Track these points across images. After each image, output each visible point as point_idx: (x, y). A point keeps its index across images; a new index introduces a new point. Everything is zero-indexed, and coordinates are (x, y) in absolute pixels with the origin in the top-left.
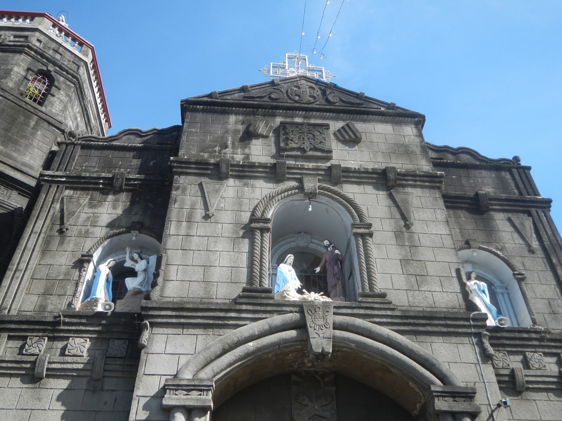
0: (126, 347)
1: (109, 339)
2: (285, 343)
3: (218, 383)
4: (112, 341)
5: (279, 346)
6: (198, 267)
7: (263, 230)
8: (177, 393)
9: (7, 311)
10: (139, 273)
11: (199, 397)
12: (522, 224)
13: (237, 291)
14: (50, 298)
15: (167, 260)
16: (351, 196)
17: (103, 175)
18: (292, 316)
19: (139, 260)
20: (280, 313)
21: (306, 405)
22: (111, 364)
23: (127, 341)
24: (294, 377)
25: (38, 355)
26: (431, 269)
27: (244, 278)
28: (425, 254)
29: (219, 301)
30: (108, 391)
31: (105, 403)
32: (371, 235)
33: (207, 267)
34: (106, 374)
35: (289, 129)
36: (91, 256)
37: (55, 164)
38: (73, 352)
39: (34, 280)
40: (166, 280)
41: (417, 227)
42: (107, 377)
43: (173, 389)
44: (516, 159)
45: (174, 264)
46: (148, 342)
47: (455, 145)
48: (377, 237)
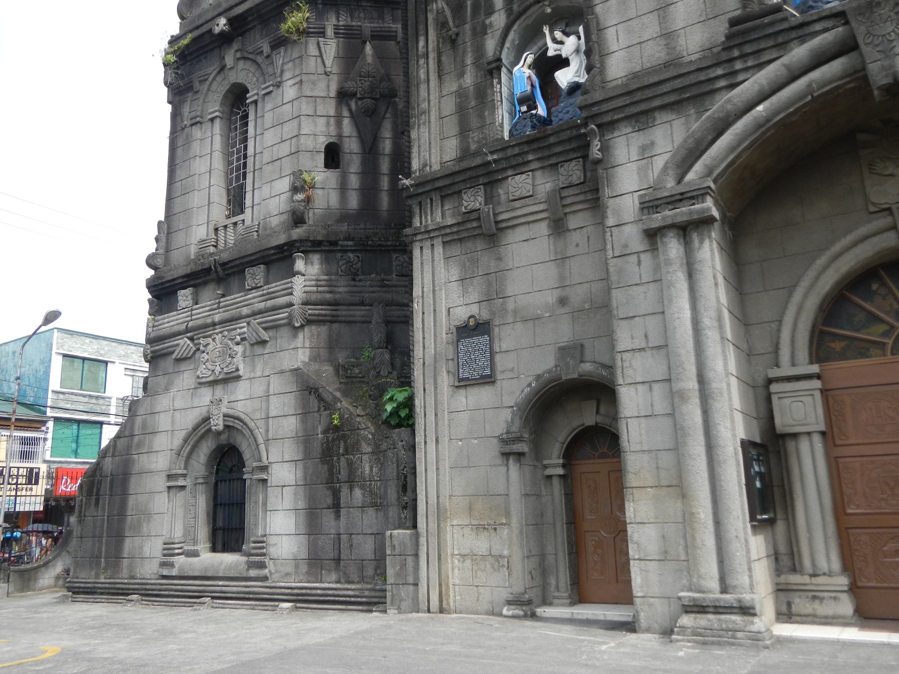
0: (581, 168)
1: (556, 164)
2: (822, 87)
3: (720, 181)
4: (561, 166)
5: (812, 96)
6: (647, 15)
8: (658, 210)
9: (428, 168)
10: (570, 58)
11: (692, 207)
13: (720, 29)
14: (469, 135)
15: (598, 24)
19: (565, 38)
21: (892, 175)
22: (569, 196)
23: (581, 160)
24: (861, 137)
25: (479, 209)
29: (693, 58)
30: (575, 229)
31: (577, 245)
34: (568, 210)
36: (499, 60)
38: (517, 195)
39: (444, 119)
42: (569, 213)
43: (652, 207)
45: (610, 25)
46: (602, 154)
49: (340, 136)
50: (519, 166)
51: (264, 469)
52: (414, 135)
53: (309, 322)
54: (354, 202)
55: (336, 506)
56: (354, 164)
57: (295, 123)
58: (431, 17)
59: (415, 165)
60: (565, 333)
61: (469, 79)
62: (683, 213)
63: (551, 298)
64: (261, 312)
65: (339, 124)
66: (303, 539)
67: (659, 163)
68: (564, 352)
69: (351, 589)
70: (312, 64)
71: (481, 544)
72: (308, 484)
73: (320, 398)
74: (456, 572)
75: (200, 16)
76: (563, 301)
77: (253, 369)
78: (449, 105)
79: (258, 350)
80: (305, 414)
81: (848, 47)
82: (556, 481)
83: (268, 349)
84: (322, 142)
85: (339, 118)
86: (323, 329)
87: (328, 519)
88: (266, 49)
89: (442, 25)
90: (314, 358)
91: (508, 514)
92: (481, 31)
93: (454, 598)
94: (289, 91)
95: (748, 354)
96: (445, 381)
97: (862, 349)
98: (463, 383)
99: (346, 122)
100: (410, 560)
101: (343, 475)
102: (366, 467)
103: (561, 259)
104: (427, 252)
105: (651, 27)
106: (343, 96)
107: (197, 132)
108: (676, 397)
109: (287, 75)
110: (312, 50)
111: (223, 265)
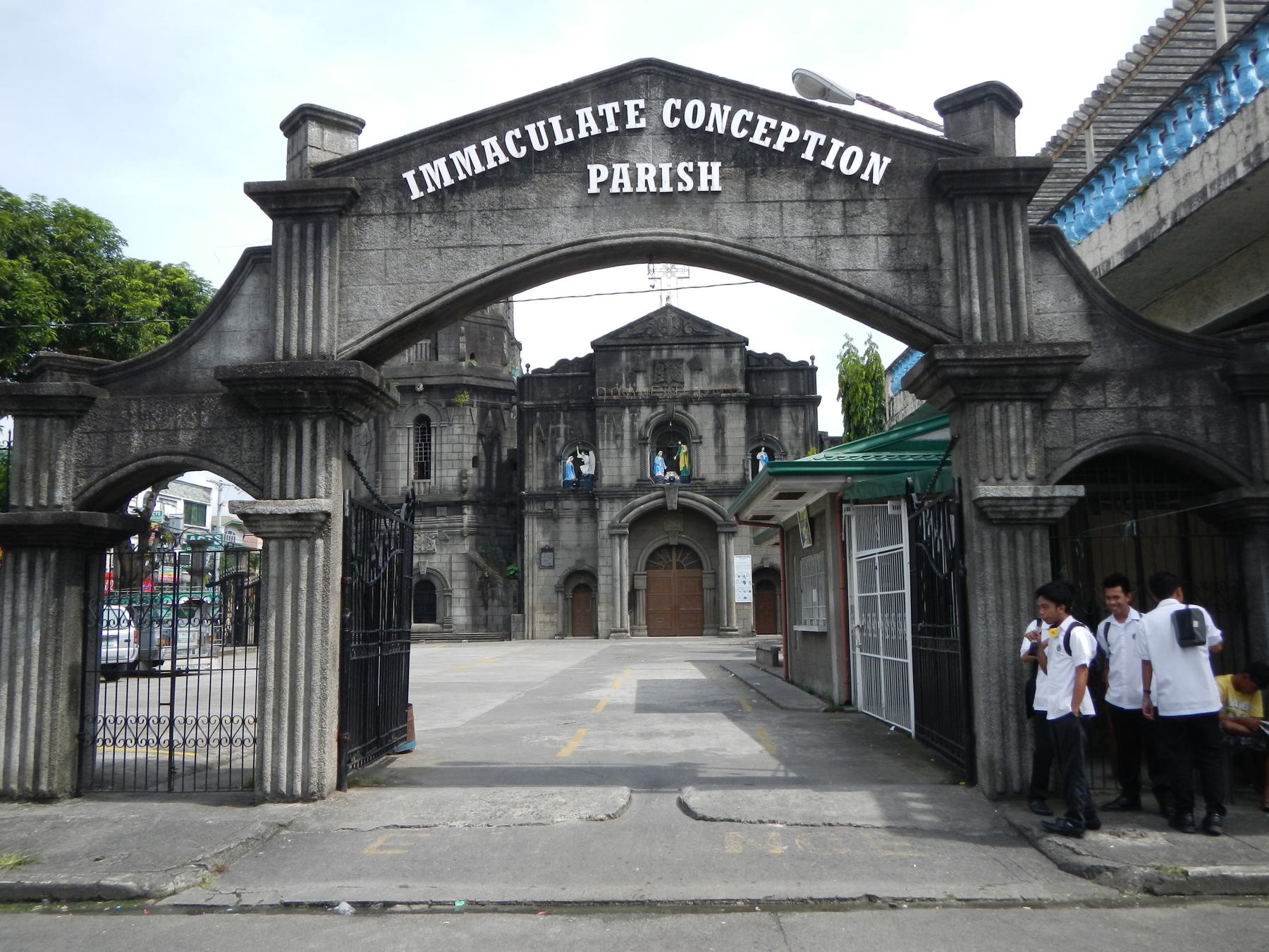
7: (646, 444)
12: (797, 417)
16: (692, 416)
17: (555, 402)
18: (659, 493)
20: (655, 491)
26: (730, 460)
27: (638, 472)
28: (729, 452)
32: (701, 443)
33: (620, 467)
35: (658, 365)
37: (526, 395)
40: (602, 476)
41: (728, 434)
44: (812, 358)
47: (770, 353)
48: (705, 442)
49: (478, 453)
50: (567, 498)
51: (451, 591)
52: (526, 474)
53: (470, 534)
54: (483, 483)
55: (486, 606)
56: (483, 467)
57: (460, 446)
58: (534, 429)
59: (526, 486)
60: (579, 555)
61: (549, 459)
62: (620, 531)
63: (575, 543)
64: (446, 527)
65: (478, 448)
66: (470, 618)
67: (615, 514)
68: (578, 561)
69: (493, 634)
70: (468, 419)
71: (547, 618)
72: (472, 598)
73: (477, 565)
74: (538, 627)
75: (397, 369)
76: (579, 545)
77: (442, 550)
78: (541, 467)
79: (444, 543)
80: (470, 571)
81: (663, 496)
82: (570, 602)
83: (450, 542)
84: (472, 455)
85: (478, 444)
86: (473, 537)
87: (482, 611)
88: (444, 405)
89: (539, 433)
90: (471, 549)
91: (557, 609)
92: (555, 442)
93: (537, 635)
94: (457, 430)
95: (630, 566)
96: (536, 566)
97: (657, 568)
98: (542, 567)
99: (481, 447)
100: (521, 625)
101: (490, 594)
102: (500, 592)
103: (579, 531)
104: (530, 521)
105: (616, 473)
106: (480, 436)
107: (400, 433)
108: (614, 580)
109: (455, 421)
110: (468, 413)
111: (425, 503)
